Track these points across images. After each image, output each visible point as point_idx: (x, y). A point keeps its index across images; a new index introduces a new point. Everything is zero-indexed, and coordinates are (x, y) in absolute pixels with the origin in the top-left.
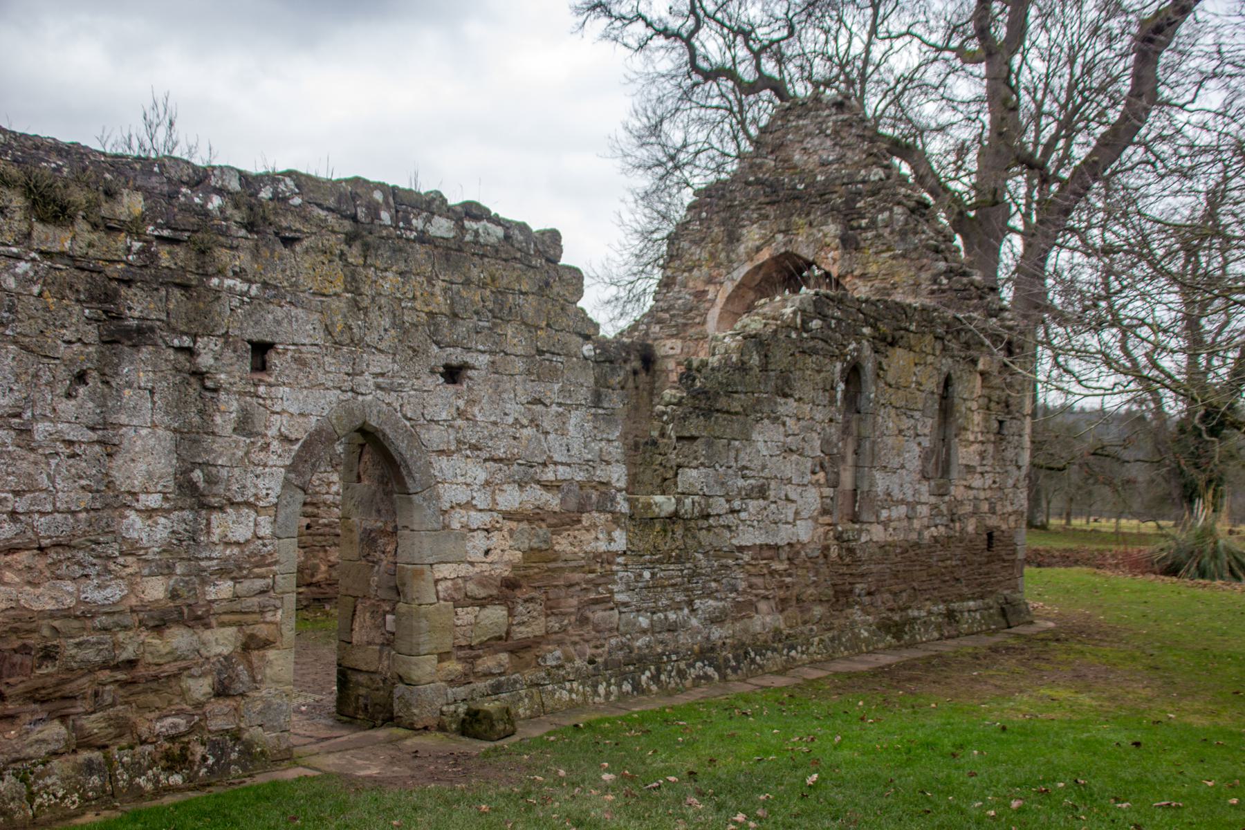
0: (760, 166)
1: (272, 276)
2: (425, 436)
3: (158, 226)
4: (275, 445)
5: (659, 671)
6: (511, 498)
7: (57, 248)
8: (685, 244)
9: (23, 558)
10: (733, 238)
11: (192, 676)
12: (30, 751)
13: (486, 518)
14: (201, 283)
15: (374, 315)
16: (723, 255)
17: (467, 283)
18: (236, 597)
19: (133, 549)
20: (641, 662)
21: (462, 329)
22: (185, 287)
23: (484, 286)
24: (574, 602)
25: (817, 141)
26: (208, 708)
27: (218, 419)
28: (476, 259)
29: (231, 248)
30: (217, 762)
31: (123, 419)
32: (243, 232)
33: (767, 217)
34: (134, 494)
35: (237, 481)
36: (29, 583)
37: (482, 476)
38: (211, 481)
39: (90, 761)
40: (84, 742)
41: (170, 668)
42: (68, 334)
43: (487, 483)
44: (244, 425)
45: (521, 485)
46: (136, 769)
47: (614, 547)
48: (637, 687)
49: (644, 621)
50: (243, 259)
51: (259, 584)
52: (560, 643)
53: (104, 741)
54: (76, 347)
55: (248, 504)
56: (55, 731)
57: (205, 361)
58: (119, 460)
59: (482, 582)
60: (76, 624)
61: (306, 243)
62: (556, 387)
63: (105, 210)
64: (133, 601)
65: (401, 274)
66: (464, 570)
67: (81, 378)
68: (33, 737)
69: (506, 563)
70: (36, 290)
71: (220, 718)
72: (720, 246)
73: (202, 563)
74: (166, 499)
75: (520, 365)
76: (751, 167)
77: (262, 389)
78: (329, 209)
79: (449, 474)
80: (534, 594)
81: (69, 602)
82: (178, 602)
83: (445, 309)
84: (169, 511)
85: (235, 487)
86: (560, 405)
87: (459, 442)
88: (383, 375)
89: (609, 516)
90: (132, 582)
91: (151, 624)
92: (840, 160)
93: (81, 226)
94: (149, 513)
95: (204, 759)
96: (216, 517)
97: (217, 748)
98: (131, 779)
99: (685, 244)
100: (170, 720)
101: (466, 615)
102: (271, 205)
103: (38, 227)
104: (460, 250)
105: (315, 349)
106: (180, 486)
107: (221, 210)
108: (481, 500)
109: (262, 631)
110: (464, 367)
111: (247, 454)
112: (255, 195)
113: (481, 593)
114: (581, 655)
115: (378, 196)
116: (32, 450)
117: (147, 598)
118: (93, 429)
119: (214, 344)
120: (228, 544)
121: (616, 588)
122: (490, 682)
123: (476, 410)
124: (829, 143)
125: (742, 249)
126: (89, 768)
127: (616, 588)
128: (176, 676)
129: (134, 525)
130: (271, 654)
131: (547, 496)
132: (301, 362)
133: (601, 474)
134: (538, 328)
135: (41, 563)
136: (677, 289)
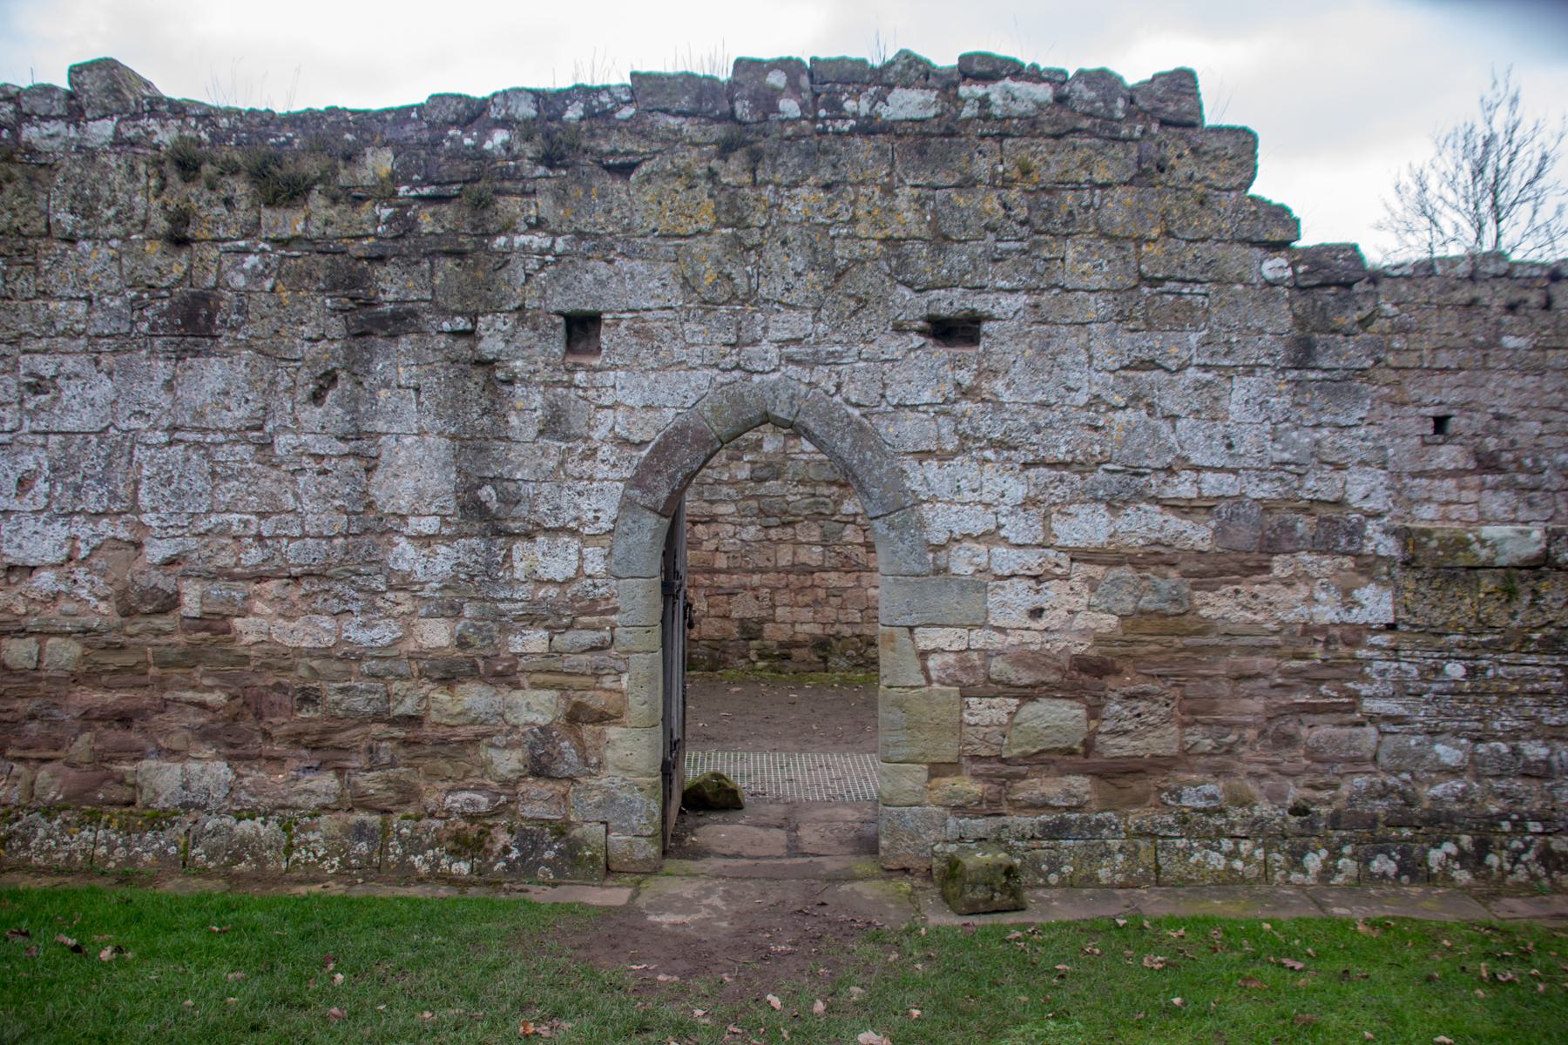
1: (593, 220)
2: (887, 430)
3: (414, 185)
4: (605, 451)
5: (1483, 847)
7: (288, 233)
9: (272, 586)
11: (493, 746)
12: (300, 800)
13: (1032, 559)
14: (480, 246)
15: (774, 255)
17: (967, 184)
18: (553, 653)
19: (404, 584)
20: (1438, 824)
21: (958, 258)
22: (459, 254)
23: (1008, 184)
24: (1257, 705)
26: (523, 788)
27: (514, 420)
28: (988, 144)
29: (524, 194)
30: (522, 859)
31: (381, 426)
32: (541, 170)
34: (403, 517)
35: (543, 501)
36: (281, 615)
38: (510, 500)
39: (363, 824)
40: (362, 802)
41: (465, 732)
42: (307, 330)
43: (1029, 503)
44: (554, 424)
46: (414, 845)
47: (1357, 616)
48: (1413, 868)
49: (1447, 753)
50: (544, 205)
51: (588, 637)
52: (1219, 772)
53: (385, 805)
54: (322, 345)
55: (563, 530)
56: (327, 782)
57: (490, 345)
58: (378, 477)
59: (1022, 658)
60: (338, 666)
61: (644, 168)
62: (1194, 338)
63: (344, 178)
64: (412, 647)
65: (827, 187)
66: (979, 639)
68: (301, 785)
69: (1083, 632)
70: (268, 284)
71: (537, 802)
73: (502, 606)
74: (444, 521)
75: (1097, 306)
77: (580, 377)
78: (685, 115)
79: (944, 488)
80: (1149, 686)
81: (328, 640)
82: (469, 652)
83: (924, 231)
84: (451, 538)
85: (543, 508)
86: (1206, 368)
87: (964, 437)
88: (798, 341)
89: (1348, 562)
90: (407, 621)
91: (437, 675)
93: (317, 201)
94: (425, 540)
95: (506, 850)
96: (519, 548)
97: (529, 840)
98: (406, 854)
100: (466, 795)
101: (987, 712)
102: (584, 126)
103: (267, 213)
104: (950, 133)
105: (669, 314)
106: (463, 508)
107: (507, 146)
108: (1016, 528)
109: (597, 700)
111: (562, 464)
112: (558, 116)
113: (1026, 677)
114: (1275, 796)
115: (777, 79)
116: (275, 466)
117: (426, 644)
118: (343, 439)
119: (504, 323)
120: (541, 582)
121: (1365, 689)
122: (1044, 818)
123: (999, 385)
126: (360, 831)
127: (1365, 689)
128: (475, 741)
129: (405, 555)
130: (613, 732)
131: (1175, 523)
132: (643, 334)
133: (1317, 485)
134: (1140, 241)
135: (295, 593)
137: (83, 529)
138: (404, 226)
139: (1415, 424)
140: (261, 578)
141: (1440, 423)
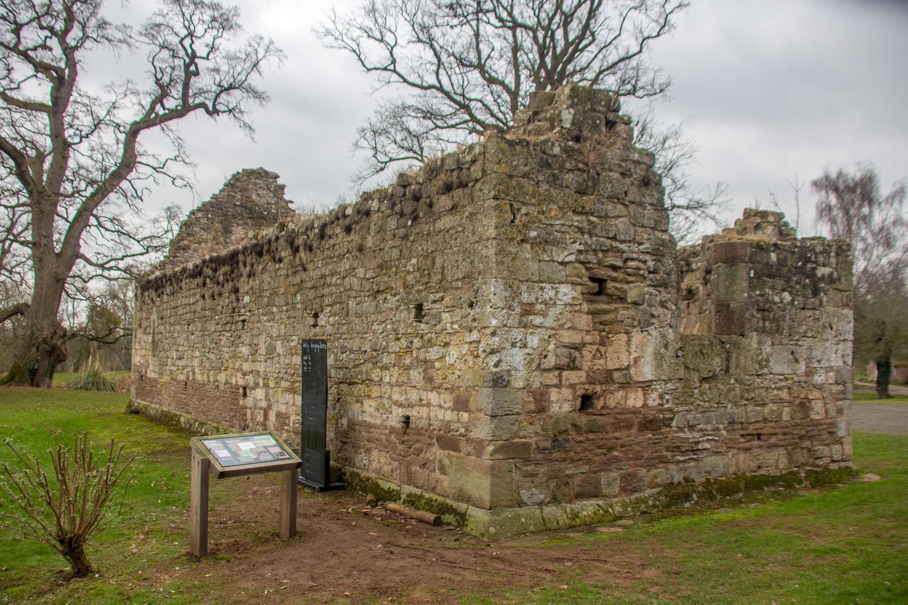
0: (233, 197)
8: (197, 229)
10: (227, 231)
16: (222, 239)
25: (265, 192)
33: (247, 224)
72: (220, 234)
76: (228, 196)
92: (276, 204)
99: (197, 229)
124: (271, 195)
125: (233, 237)
136: (190, 252)
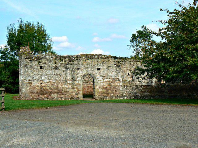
6: (106, 80)
9: (60, 84)
13: (103, 82)
37: (102, 78)
38: (74, 78)
44: (77, 74)
45: (107, 79)
67: (64, 71)
93: (63, 61)
96: (75, 81)
101: (101, 90)
110: (100, 69)
129: (68, 82)
131: (110, 80)
132: (82, 69)
133: (118, 78)
137: (49, 80)
138: (69, 63)
139: (126, 74)
140: (60, 83)
141: (128, 74)
